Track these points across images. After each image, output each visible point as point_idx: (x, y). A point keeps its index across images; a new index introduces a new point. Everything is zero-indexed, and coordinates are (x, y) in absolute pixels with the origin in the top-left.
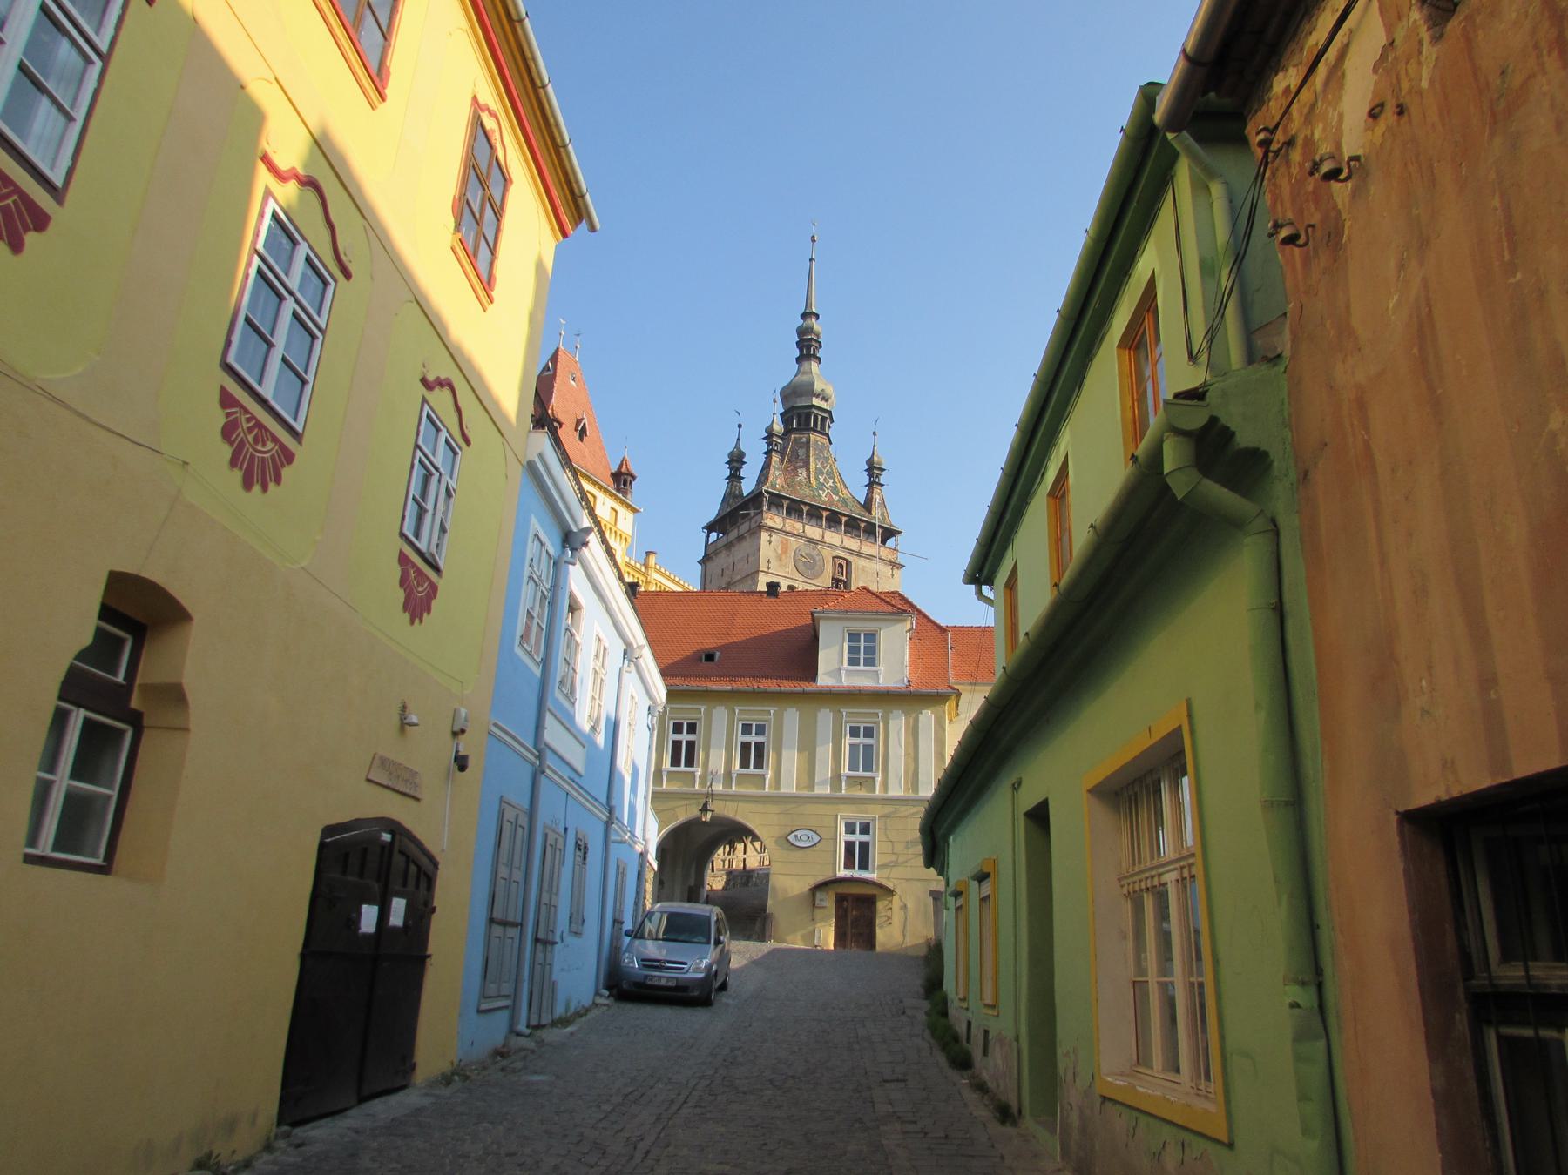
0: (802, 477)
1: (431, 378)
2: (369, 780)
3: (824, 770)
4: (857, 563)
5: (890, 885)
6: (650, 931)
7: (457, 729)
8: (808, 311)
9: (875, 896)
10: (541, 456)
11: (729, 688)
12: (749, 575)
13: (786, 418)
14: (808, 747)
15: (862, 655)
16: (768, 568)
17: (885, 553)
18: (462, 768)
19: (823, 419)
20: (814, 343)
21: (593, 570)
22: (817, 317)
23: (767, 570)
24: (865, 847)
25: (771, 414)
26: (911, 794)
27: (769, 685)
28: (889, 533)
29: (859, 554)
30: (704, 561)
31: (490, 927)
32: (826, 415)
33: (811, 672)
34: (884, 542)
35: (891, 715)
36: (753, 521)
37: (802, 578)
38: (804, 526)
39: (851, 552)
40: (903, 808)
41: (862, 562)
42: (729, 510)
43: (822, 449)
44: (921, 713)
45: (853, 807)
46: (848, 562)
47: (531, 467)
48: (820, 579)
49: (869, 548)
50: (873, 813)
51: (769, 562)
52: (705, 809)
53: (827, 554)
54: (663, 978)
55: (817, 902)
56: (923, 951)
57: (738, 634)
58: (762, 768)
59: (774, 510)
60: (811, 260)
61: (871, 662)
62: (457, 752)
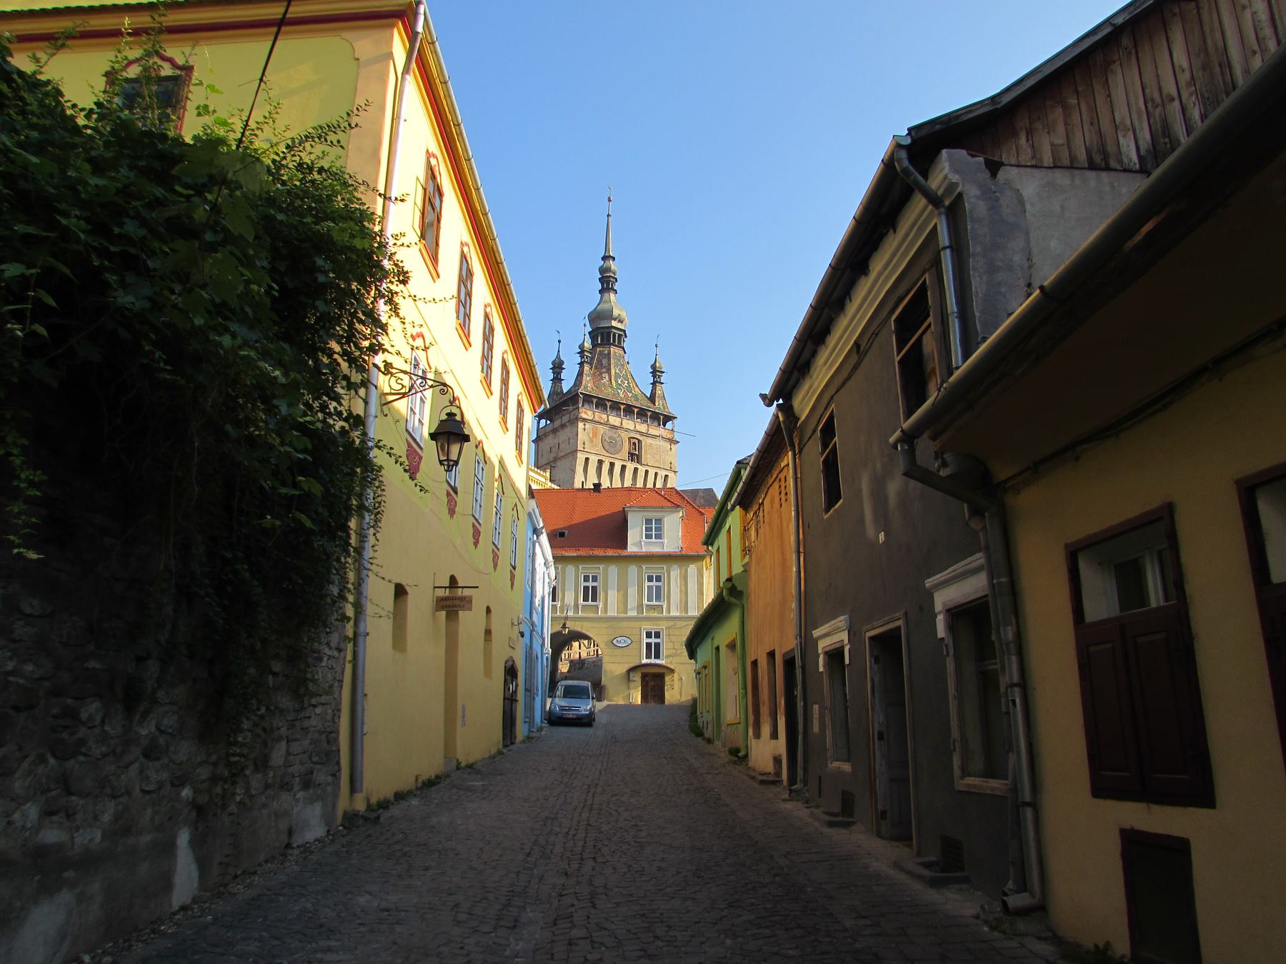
0: (606, 380)
3: (632, 602)
4: (646, 442)
5: (672, 667)
8: (607, 254)
9: (664, 673)
10: (533, 510)
11: (575, 554)
12: (569, 454)
13: (593, 335)
14: (623, 588)
16: (584, 448)
19: (620, 335)
20: (612, 279)
24: (657, 645)
25: (580, 334)
26: (684, 614)
27: (599, 552)
28: (668, 418)
29: (647, 435)
32: (622, 333)
33: (623, 543)
34: (664, 425)
35: (671, 569)
36: (572, 414)
37: (608, 454)
40: (680, 623)
41: (649, 441)
46: (639, 441)
47: (530, 514)
48: (620, 454)
49: (653, 431)
51: (584, 444)
52: (564, 626)
53: (625, 436)
54: (571, 714)
55: (631, 678)
56: (691, 703)
57: (578, 518)
58: (596, 601)
59: (586, 406)
61: (659, 536)
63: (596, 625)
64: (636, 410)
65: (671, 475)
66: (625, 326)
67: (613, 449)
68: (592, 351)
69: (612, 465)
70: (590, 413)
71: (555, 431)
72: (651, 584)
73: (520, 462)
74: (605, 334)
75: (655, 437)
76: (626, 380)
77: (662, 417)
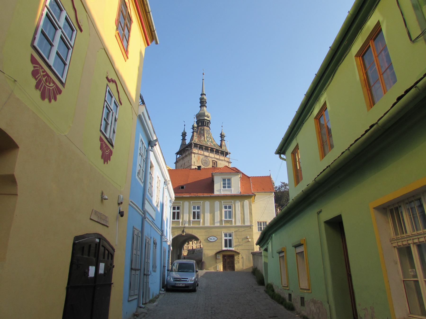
0: (203, 139)
1: (110, 78)
2: (91, 219)
3: (217, 219)
4: (219, 162)
5: (238, 251)
6: (174, 269)
7: (119, 202)
8: (202, 93)
9: (234, 255)
10: (143, 113)
11: (189, 196)
13: (197, 123)
14: (212, 212)
15: (227, 185)
16: (194, 164)
17: (226, 159)
18: (122, 216)
19: (208, 123)
20: (204, 102)
21: (157, 155)
22: (205, 95)
23: (194, 165)
24: (230, 240)
25: (193, 121)
26: (243, 225)
28: (227, 154)
29: (219, 160)
30: (176, 163)
31: (131, 271)
32: (209, 122)
33: (212, 191)
34: (226, 156)
36: (190, 151)
38: (204, 152)
39: (217, 159)
40: (241, 229)
42: (183, 148)
43: (208, 131)
44: (245, 201)
45: (226, 229)
46: (216, 162)
47: (140, 117)
49: (222, 158)
50: (232, 231)
51: (194, 162)
52: (183, 232)
53: (211, 160)
54: (181, 284)
55: (217, 257)
56: (251, 270)
58: (199, 219)
59: (195, 148)
60: (203, 79)
61: (229, 187)
62: (120, 210)
63: (199, 230)
68: (197, 127)
71: (183, 158)
72: (226, 210)
73: (126, 57)
74: (202, 122)
75: (222, 160)
76: (211, 139)
77: (225, 153)
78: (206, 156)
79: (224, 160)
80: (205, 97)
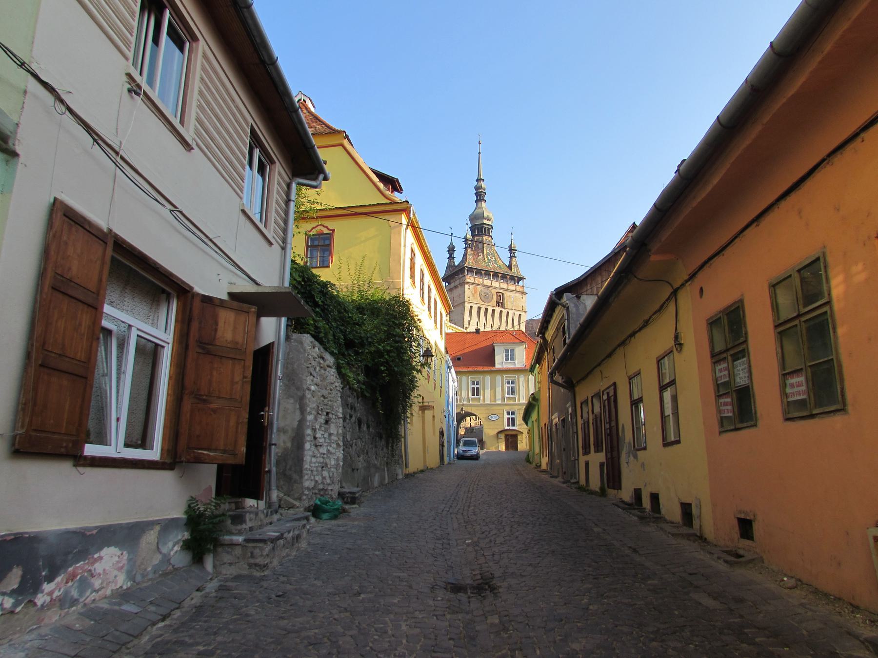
0: (481, 257)
3: (499, 396)
4: (507, 294)
5: (522, 431)
14: (493, 388)
19: (489, 229)
24: (513, 419)
25: (464, 230)
27: (480, 369)
28: (520, 279)
29: (507, 290)
32: (490, 227)
33: (493, 364)
34: (518, 283)
35: (520, 377)
36: (461, 279)
39: (503, 289)
41: (509, 293)
45: (508, 407)
46: (503, 294)
47: (446, 361)
48: (491, 303)
49: (512, 287)
50: (515, 409)
52: (462, 410)
53: (494, 291)
54: (468, 454)
55: (499, 437)
58: (479, 395)
59: (470, 274)
60: (479, 153)
61: (513, 359)
63: (479, 408)
64: (500, 275)
65: (523, 314)
66: (492, 222)
67: (487, 300)
69: (486, 310)
70: (472, 278)
72: (509, 385)
77: (516, 279)
78: (487, 286)
79: (514, 289)
80: (483, 184)
